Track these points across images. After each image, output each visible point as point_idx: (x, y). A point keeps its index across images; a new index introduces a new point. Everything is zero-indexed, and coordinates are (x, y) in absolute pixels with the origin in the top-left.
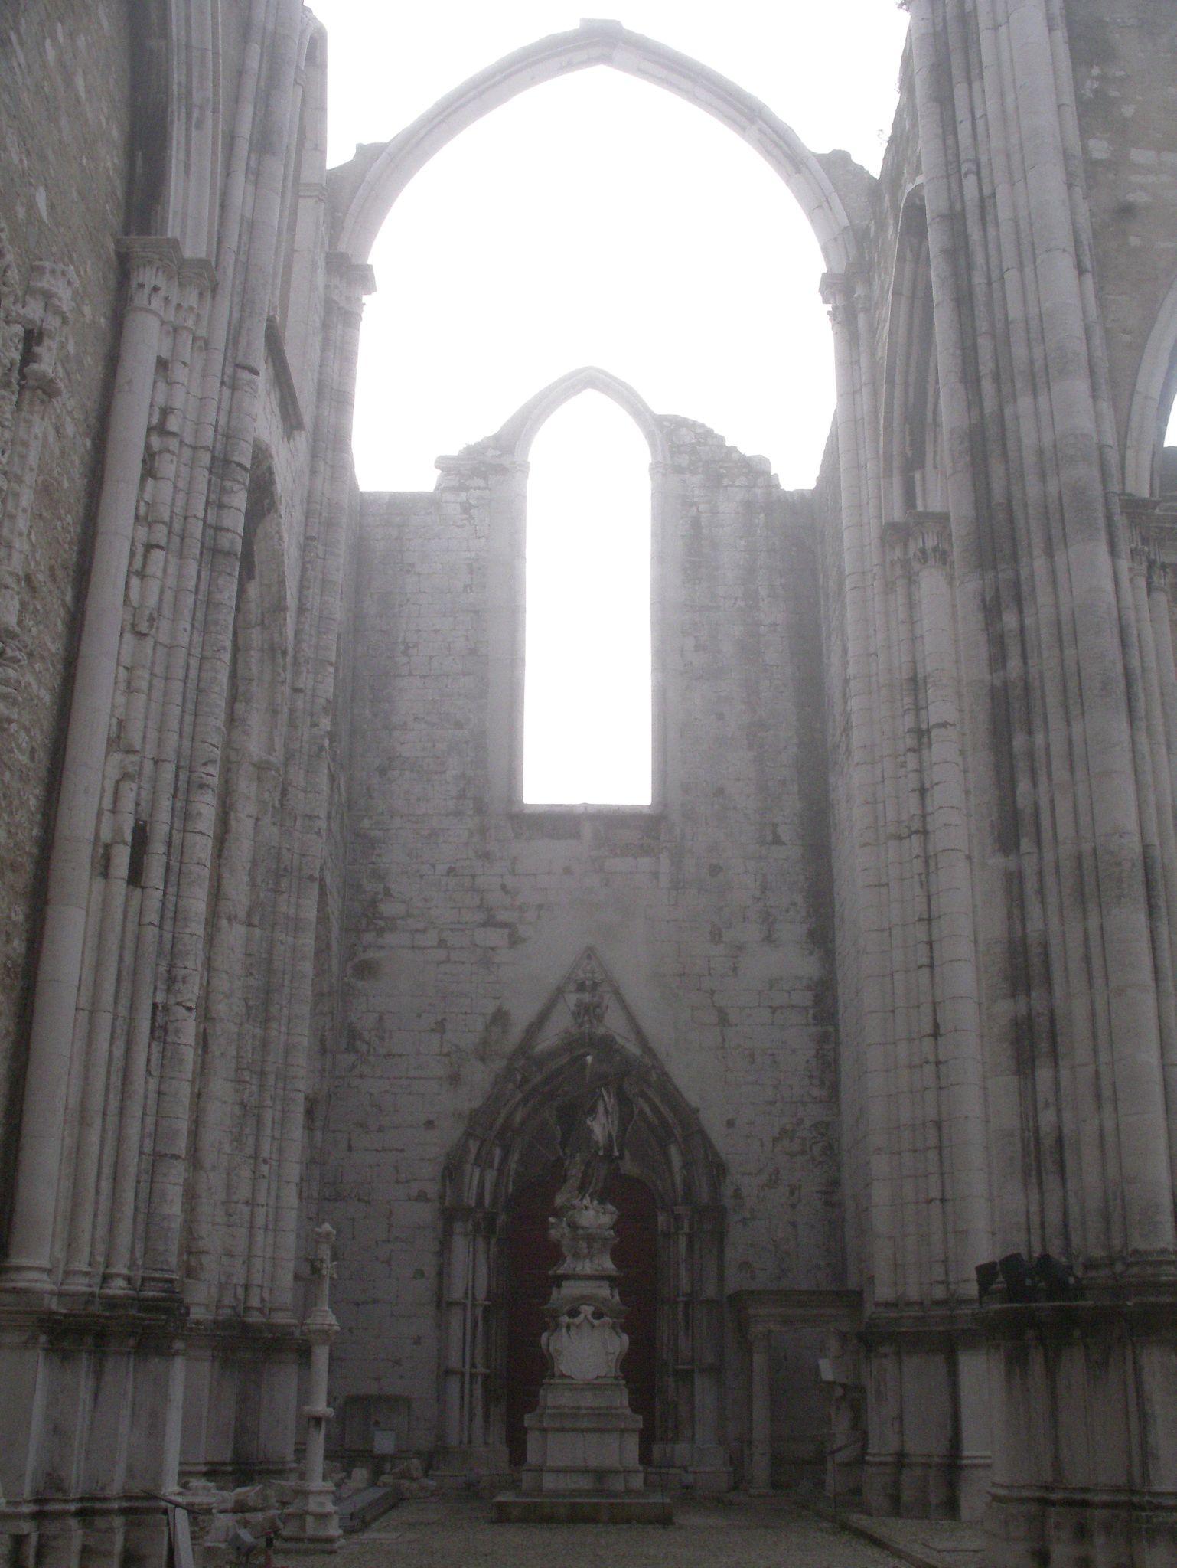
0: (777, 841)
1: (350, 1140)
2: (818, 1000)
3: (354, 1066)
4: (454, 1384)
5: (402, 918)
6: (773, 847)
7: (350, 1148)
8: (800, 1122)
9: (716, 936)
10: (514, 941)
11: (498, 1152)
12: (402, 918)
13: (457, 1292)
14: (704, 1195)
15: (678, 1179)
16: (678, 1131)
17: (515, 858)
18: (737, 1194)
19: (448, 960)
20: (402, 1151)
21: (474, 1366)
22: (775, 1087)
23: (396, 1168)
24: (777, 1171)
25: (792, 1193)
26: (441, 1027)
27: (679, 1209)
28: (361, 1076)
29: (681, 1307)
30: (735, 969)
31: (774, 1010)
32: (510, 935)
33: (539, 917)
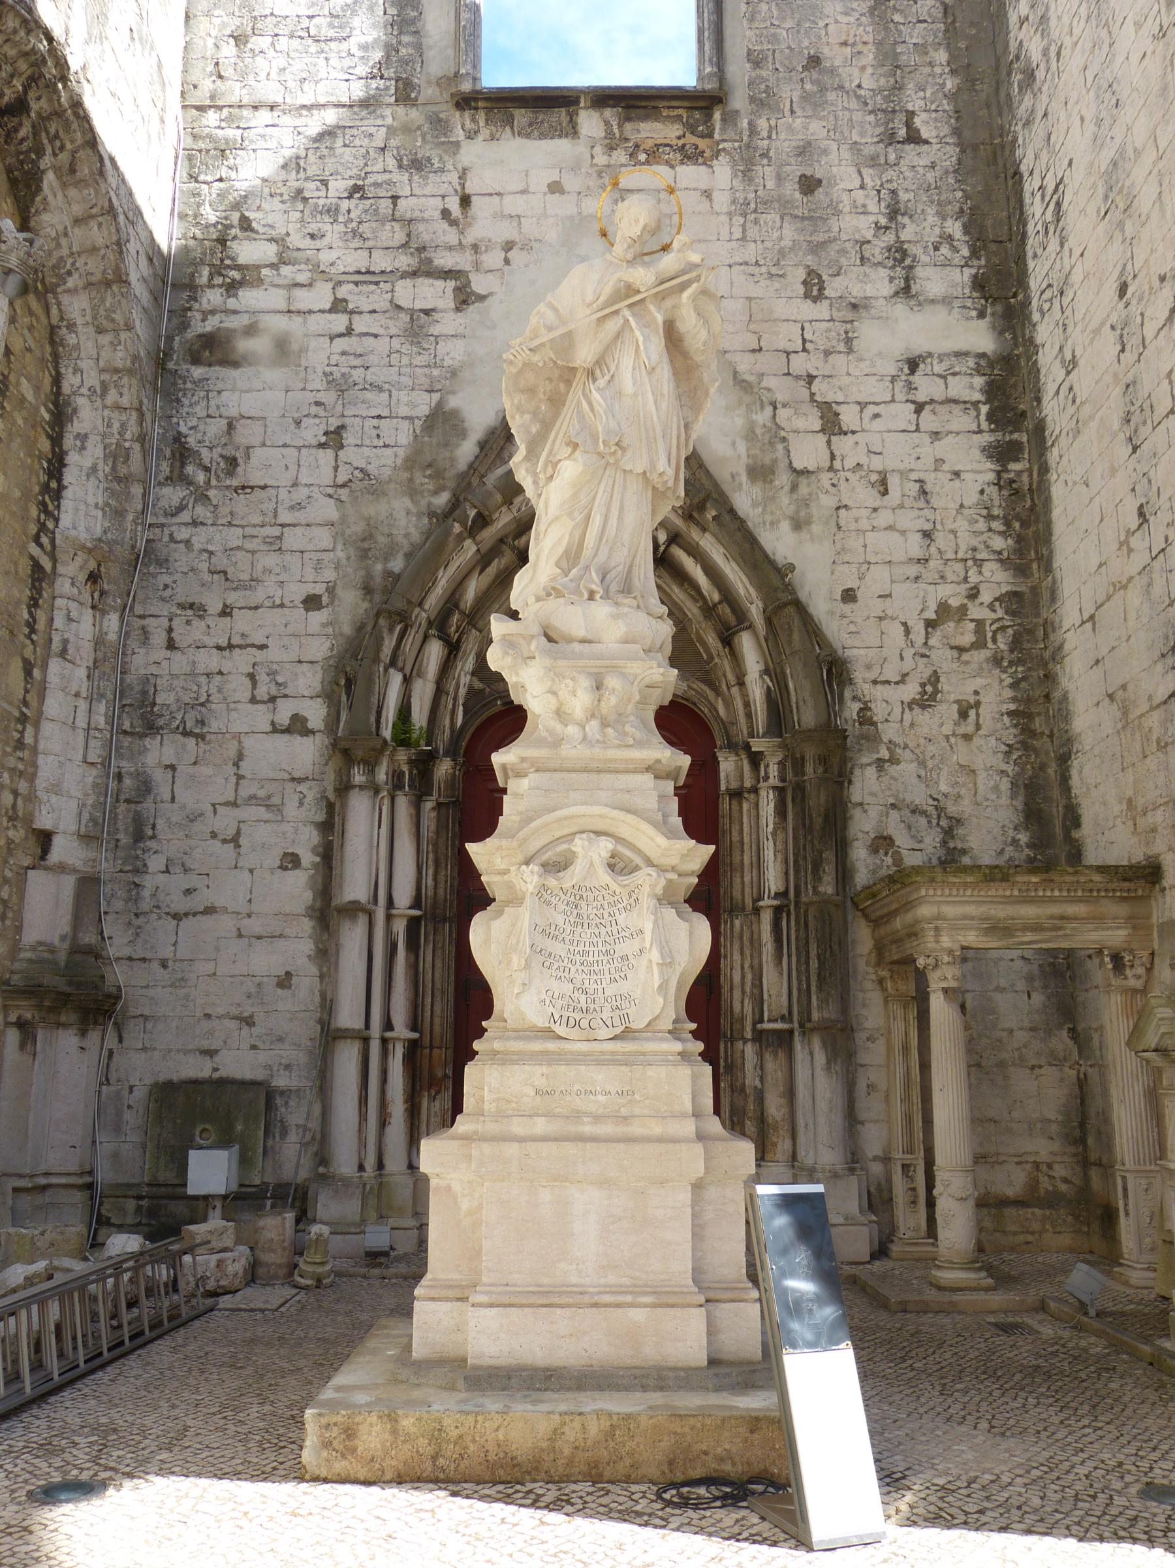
0: (914, 138)
1: (170, 630)
2: (993, 391)
3: (181, 508)
4: (347, 1060)
5: (272, 266)
6: (908, 147)
7: (171, 645)
8: (974, 594)
9: (814, 288)
10: (465, 298)
11: (435, 651)
12: (272, 266)
13: (355, 886)
14: (807, 716)
15: (757, 694)
16: (755, 611)
17: (465, 170)
18: (865, 717)
19: (349, 332)
20: (262, 647)
21: (388, 1025)
22: (927, 535)
23: (252, 676)
24: (935, 678)
25: (963, 714)
26: (334, 439)
27: (757, 745)
28: (195, 523)
29: (766, 918)
30: (848, 341)
31: (919, 408)
32: (457, 290)
33: (507, 261)
